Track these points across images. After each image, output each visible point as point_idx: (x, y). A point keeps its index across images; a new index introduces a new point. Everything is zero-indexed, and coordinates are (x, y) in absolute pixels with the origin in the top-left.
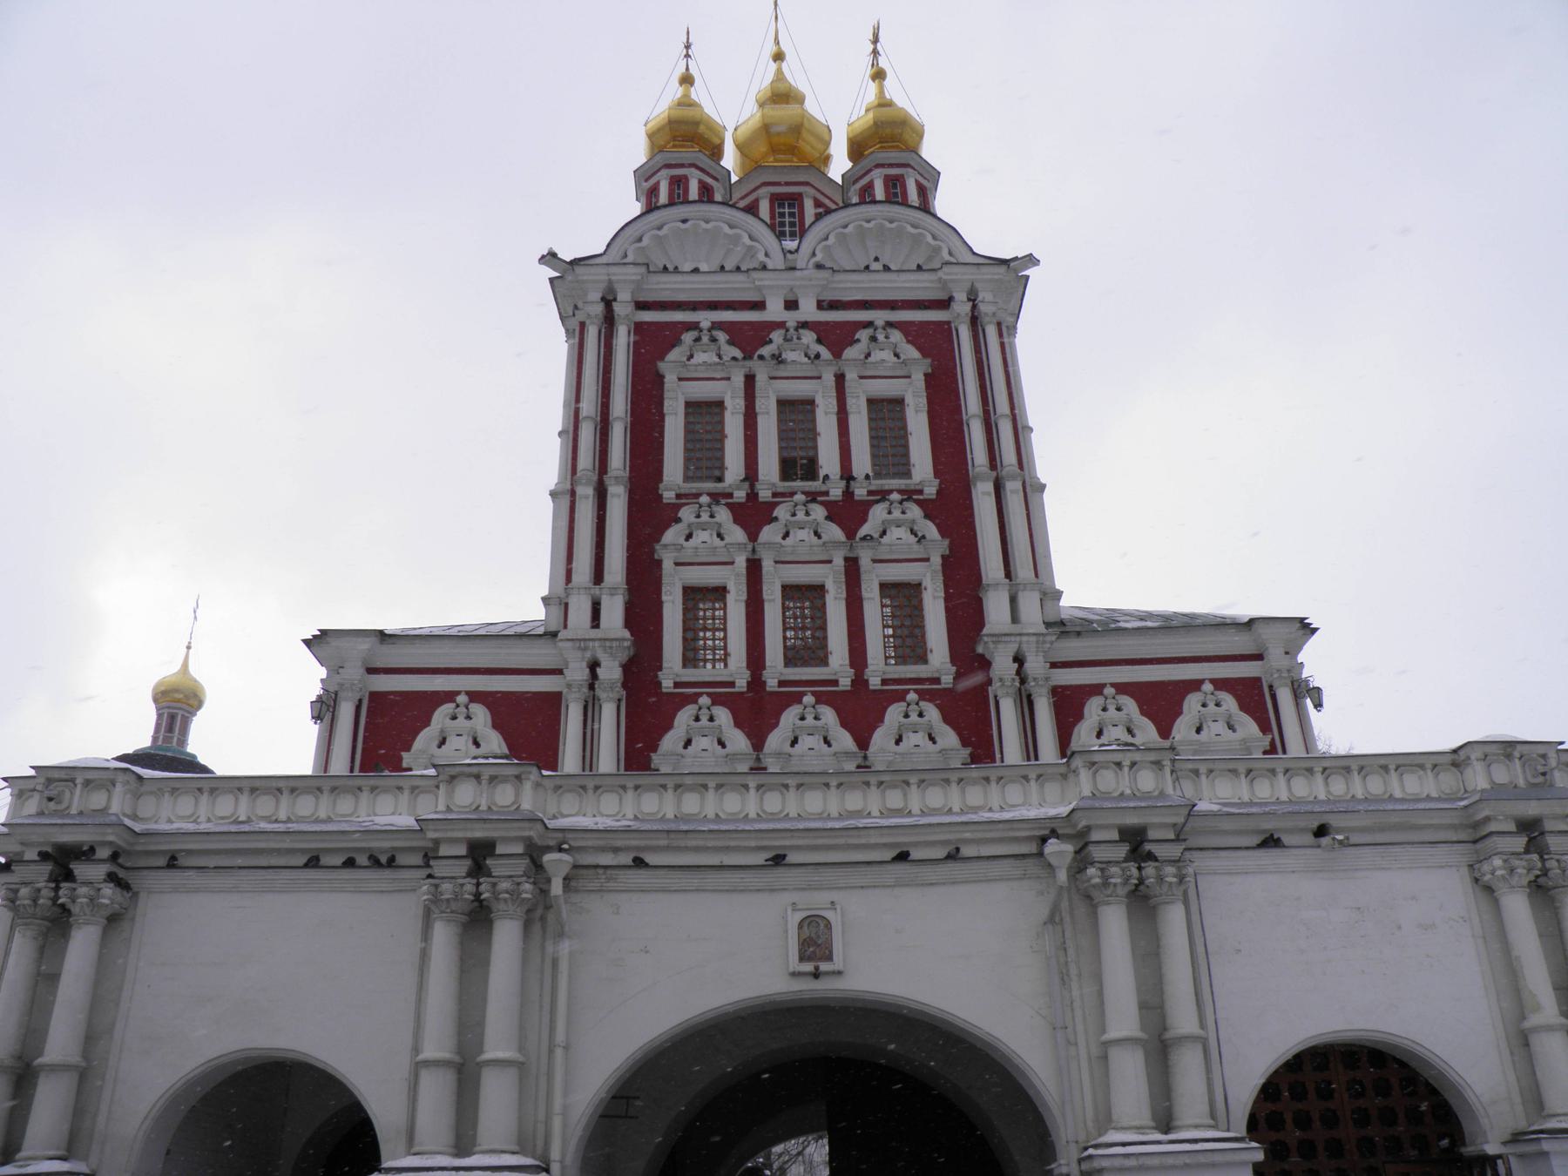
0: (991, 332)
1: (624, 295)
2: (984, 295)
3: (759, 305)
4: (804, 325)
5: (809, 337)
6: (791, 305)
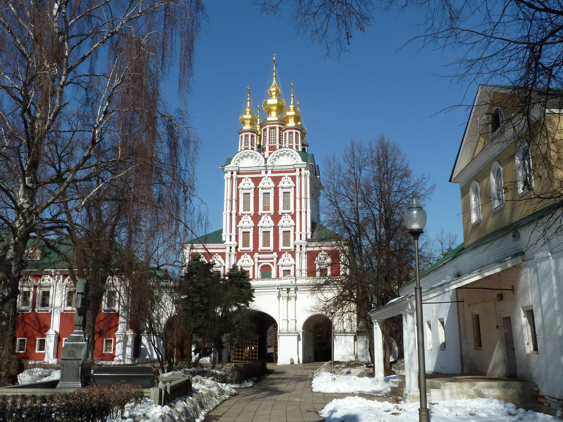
0: (303, 178)
1: (235, 173)
2: (303, 170)
3: (260, 173)
4: (268, 177)
5: (270, 179)
6: (266, 172)
